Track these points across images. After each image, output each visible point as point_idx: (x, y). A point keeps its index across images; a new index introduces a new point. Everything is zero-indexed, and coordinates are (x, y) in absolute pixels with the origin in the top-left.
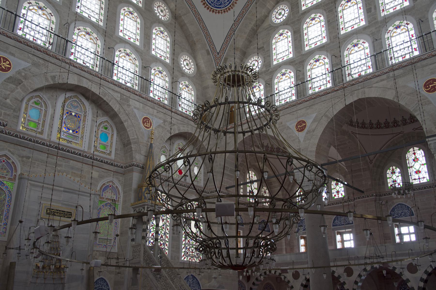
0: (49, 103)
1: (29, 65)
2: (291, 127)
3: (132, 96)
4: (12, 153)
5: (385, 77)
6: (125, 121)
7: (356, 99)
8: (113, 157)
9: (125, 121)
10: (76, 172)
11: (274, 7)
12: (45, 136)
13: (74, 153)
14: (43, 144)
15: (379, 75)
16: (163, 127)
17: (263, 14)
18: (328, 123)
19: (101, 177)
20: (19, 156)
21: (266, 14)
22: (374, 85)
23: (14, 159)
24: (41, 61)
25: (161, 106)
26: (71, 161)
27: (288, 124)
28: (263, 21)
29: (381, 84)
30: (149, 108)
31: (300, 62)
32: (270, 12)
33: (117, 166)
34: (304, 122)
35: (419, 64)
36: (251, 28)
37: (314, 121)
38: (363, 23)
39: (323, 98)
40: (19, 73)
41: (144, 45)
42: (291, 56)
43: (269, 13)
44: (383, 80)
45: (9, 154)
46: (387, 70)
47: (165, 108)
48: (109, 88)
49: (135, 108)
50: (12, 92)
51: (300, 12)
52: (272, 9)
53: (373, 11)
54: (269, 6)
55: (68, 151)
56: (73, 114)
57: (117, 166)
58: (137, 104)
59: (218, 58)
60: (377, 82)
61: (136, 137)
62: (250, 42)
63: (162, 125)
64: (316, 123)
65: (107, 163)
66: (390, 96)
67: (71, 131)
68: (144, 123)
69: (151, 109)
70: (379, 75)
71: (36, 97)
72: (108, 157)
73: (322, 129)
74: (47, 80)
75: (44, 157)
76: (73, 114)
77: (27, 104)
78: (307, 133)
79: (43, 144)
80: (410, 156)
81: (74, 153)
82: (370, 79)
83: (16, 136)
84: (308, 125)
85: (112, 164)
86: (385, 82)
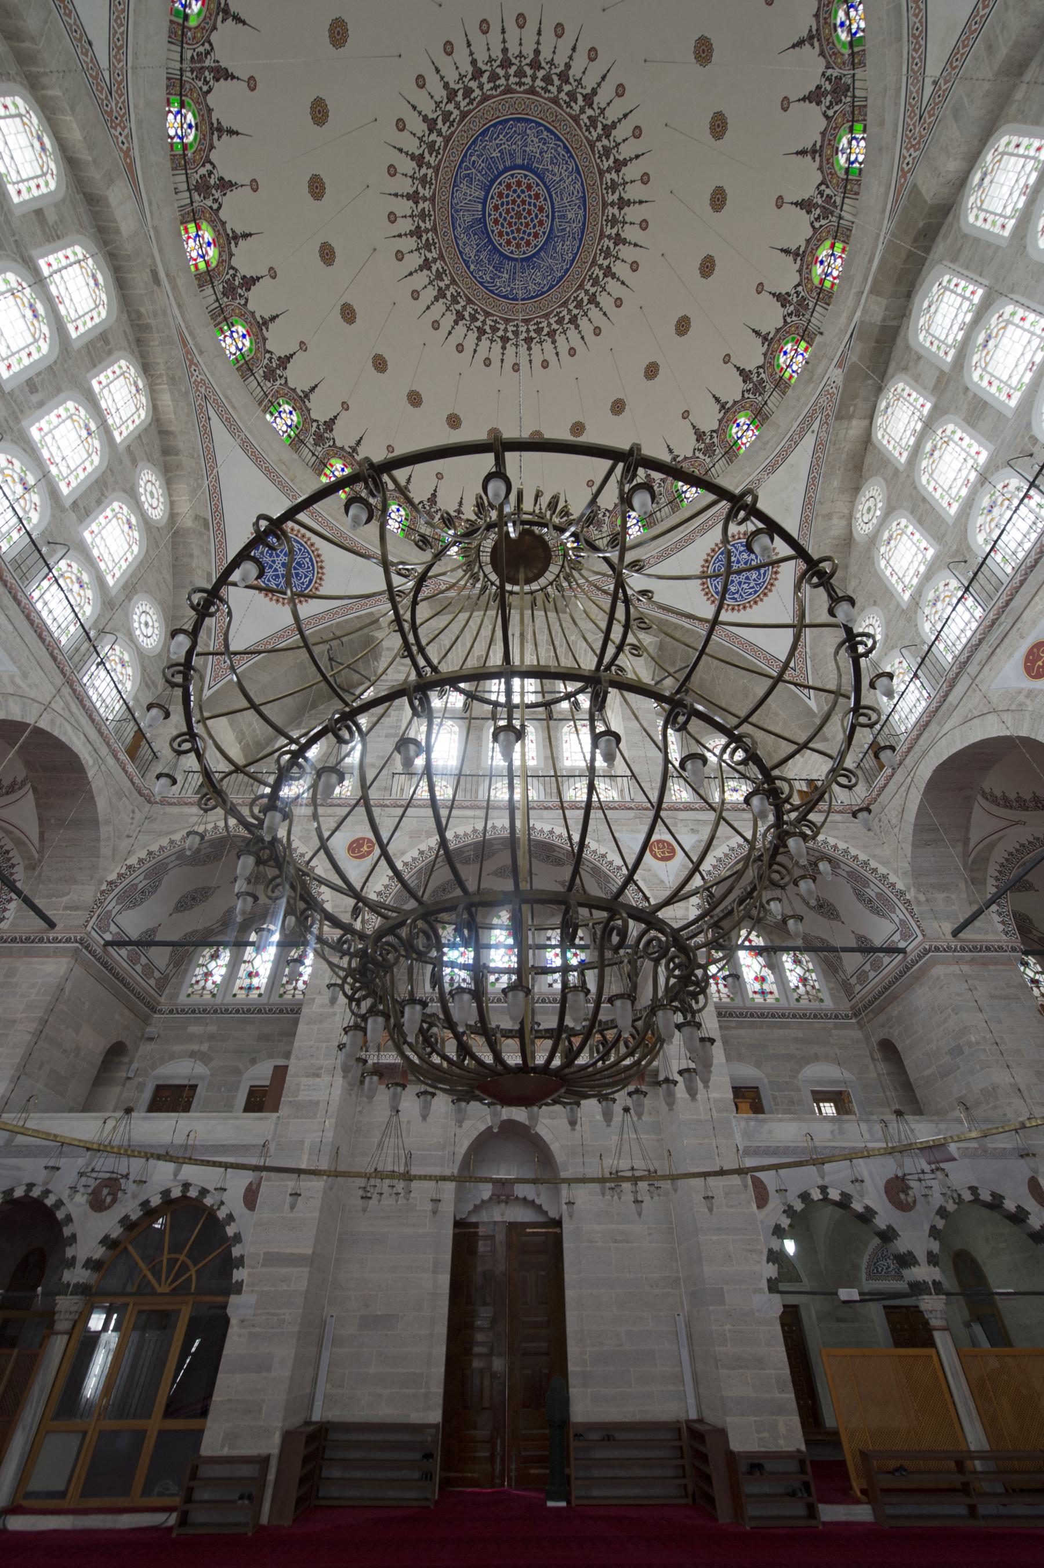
53: (35, 398)
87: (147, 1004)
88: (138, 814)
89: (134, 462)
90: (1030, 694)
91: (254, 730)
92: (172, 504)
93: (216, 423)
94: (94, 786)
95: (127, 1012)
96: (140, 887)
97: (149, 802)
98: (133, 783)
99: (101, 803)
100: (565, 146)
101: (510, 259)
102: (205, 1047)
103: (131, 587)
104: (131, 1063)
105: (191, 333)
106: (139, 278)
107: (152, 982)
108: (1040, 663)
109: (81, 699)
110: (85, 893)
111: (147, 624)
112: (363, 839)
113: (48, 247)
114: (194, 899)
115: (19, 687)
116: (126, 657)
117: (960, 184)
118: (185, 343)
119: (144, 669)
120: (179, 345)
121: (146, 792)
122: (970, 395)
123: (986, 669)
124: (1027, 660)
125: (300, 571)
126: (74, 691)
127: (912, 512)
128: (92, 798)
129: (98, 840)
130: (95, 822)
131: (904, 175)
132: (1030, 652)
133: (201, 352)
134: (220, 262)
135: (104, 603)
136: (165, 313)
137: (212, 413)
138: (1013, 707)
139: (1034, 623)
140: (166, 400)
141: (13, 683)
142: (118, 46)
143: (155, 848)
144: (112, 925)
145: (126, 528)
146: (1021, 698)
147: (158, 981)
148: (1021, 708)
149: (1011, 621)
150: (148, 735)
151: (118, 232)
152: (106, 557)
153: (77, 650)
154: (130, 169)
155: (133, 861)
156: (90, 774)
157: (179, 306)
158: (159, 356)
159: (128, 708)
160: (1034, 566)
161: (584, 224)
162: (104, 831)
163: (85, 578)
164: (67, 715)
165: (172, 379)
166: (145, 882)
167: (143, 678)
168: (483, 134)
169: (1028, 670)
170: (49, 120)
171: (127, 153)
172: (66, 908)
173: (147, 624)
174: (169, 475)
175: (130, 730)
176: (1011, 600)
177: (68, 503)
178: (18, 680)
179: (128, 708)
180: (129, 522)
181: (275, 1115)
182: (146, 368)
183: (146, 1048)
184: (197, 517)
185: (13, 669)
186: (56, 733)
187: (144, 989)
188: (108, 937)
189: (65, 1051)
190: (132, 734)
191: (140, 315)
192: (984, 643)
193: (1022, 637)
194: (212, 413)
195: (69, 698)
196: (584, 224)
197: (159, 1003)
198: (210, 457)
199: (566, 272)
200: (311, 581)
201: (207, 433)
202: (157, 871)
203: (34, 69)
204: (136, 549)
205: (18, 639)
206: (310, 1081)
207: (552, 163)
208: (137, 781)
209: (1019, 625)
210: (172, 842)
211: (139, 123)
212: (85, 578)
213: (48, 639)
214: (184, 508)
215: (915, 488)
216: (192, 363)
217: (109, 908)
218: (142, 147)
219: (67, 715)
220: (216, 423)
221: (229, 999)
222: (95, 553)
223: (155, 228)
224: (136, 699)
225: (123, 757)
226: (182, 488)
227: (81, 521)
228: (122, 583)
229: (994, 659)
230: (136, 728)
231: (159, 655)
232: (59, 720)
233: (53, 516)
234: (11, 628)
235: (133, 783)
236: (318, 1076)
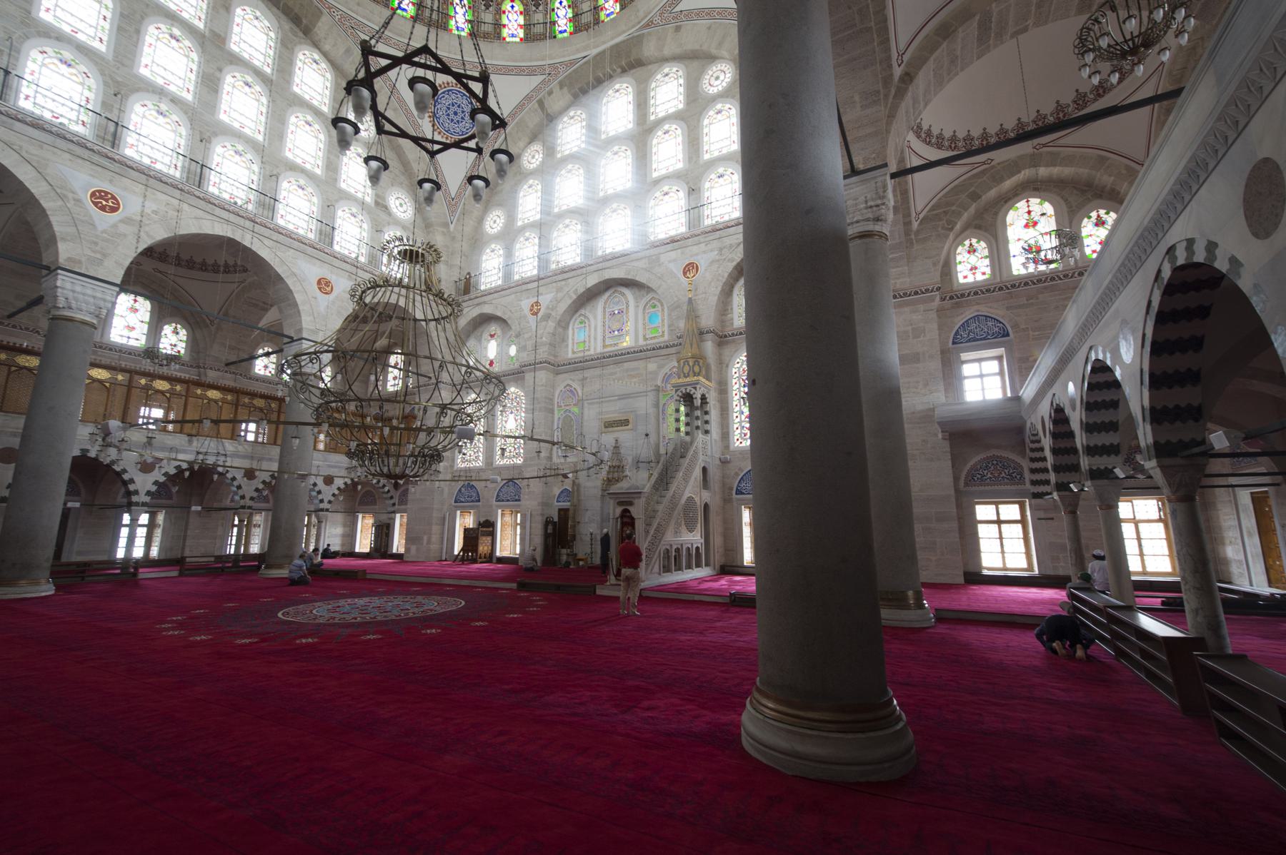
0: (591, 317)
1: (552, 294)
3: (662, 249)
4: (573, 381)
6: (659, 287)
8: (666, 337)
9: (659, 287)
10: (632, 373)
12: (592, 352)
13: (622, 354)
14: (592, 360)
16: (718, 261)
19: (661, 367)
20: (579, 380)
23: (575, 385)
24: (563, 283)
25: (710, 232)
26: (625, 364)
30: (690, 248)
33: (674, 346)
40: (548, 308)
41: (690, 159)
45: (570, 382)
47: (718, 230)
48: (632, 261)
49: (670, 262)
50: (545, 329)
55: (616, 355)
56: (616, 312)
57: (674, 346)
58: (673, 255)
61: (676, 299)
63: (717, 257)
65: (660, 348)
67: (616, 333)
68: (685, 273)
69: (695, 247)
71: (580, 316)
72: (662, 339)
74: (571, 297)
75: (597, 371)
76: (616, 312)
77: (573, 329)
79: (592, 360)
81: (622, 354)
83: (570, 364)
85: (667, 347)
90: (78, 201)
108: (104, 203)
117: (316, 45)
122: (217, 74)
123: (67, 156)
124: (100, 191)
127: (122, 15)
131: (329, 8)
132: (107, 193)
138: (59, 191)
139: (125, 189)
146: (70, 195)
148: (62, 197)
149: (117, 170)
160: (161, 181)
169: (93, 194)
176: (133, 169)
192: (91, 153)
193: (111, 181)
209: (117, 176)
215: (143, 18)
229: (80, 161)
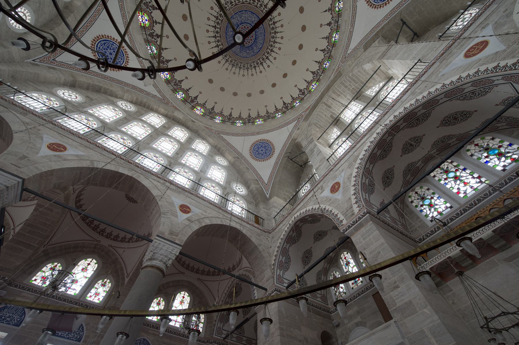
2: (44, 139)
5: (162, 181)
7: (130, 174)
11: (127, 100)
15: (160, 178)
17: (118, 93)
18: (87, 167)
21: (119, 96)
22: (151, 180)
27: (45, 136)
28: (112, 96)
29: (155, 183)
31: (109, 128)
32: (122, 99)
34: (65, 149)
35: (187, 193)
36: (101, 86)
37: (77, 156)
38: (169, 155)
39: (105, 153)
42: (108, 121)
43: (120, 98)
44: (159, 182)
46: (167, 180)
51: (140, 118)
52: (125, 100)
53: (179, 156)
54: (126, 96)
59: (49, 60)
60: (154, 180)
62: (87, 89)
64: (76, 158)
66: (155, 192)
70: (160, 178)
73: (76, 166)
78: (55, 156)
80: (83, 263)
82: (153, 174)
84: (66, 153)
86: (159, 184)
87: (324, 310)
88: (269, 239)
89: (212, 156)
91: (288, 195)
92: (228, 160)
93: (225, 137)
94: (247, 235)
95: (318, 317)
96: (283, 260)
97: (270, 233)
98: (260, 230)
99: (253, 239)
100: (239, 12)
101: (252, 44)
102: (358, 319)
103: (228, 182)
104: (337, 341)
105: (207, 125)
106: (190, 124)
107: (319, 299)
109: (231, 214)
110: (268, 273)
111: (239, 189)
112: (334, 185)
113: (168, 130)
114: (307, 257)
115: (205, 215)
116: (238, 199)
118: (207, 128)
119: (246, 200)
120: (206, 129)
121: (266, 230)
125: (267, 148)
126: (223, 210)
128: (250, 239)
129: (260, 252)
130: (256, 247)
133: (211, 127)
134: (205, 110)
135: (222, 188)
136: (199, 126)
137: (222, 135)
140: (211, 140)
141: (203, 215)
142: (159, 92)
143: (278, 244)
144: (284, 280)
145: (219, 170)
147: (321, 298)
150: (259, 215)
151: (180, 119)
152: (217, 178)
153: (221, 202)
154: (176, 108)
155: (275, 253)
156: (244, 232)
157: (201, 122)
158: (203, 134)
159: (247, 211)
161: (257, 16)
162: (260, 248)
163: (214, 185)
164: (225, 217)
165: (209, 136)
166: (284, 258)
167: (247, 202)
168: (226, 34)
170: (158, 113)
171: (173, 106)
172: (267, 281)
173: (239, 189)
174: (222, 154)
175: (253, 218)
177: (199, 171)
178: (204, 213)
179: (247, 211)
180: (219, 169)
181: (392, 321)
182: (203, 138)
183: (339, 331)
184: (234, 158)
185: (201, 211)
186: (224, 224)
187: (317, 303)
188: (286, 285)
189: (300, 341)
190: (254, 218)
191: (194, 130)
194: (222, 135)
195: (223, 213)
196: (257, 16)
197: (329, 308)
198: (228, 144)
199: (264, 29)
200: (271, 148)
201: (224, 140)
202: (284, 251)
203: (151, 107)
204: (225, 174)
205: (199, 203)
206: (396, 292)
207: (240, 18)
208: (261, 228)
210: (281, 239)
211: (171, 99)
212: (214, 185)
213: (206, 199)
214: (230, 158)
216: (211, 130)
217: (278, 273)
218: (175, 103)
219: (225, 217)
220: (225, 137)
221: (352, 291)
222: (213, 179)
223: (187, 114)
224: (249, 208)
225: (256, 225)
226: (227, 154)
227: (205, 173)
228: (225, 182)
230: (254, 216)
231: (248, 194)
232: (223, 220)
233: (197, 175)
234: (195, 202)
235: (260, 230)
236: (398, 287)
